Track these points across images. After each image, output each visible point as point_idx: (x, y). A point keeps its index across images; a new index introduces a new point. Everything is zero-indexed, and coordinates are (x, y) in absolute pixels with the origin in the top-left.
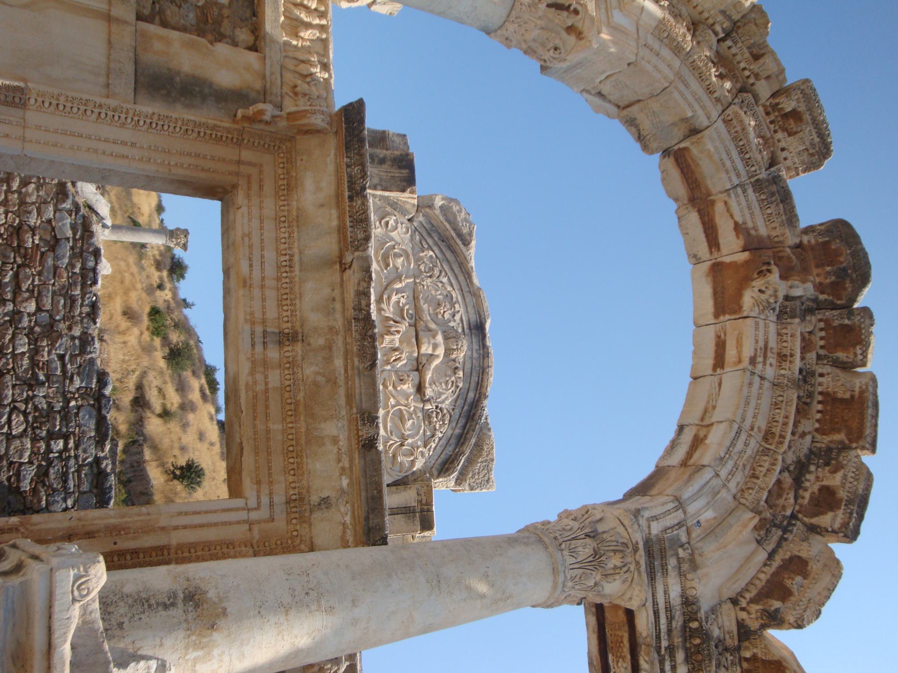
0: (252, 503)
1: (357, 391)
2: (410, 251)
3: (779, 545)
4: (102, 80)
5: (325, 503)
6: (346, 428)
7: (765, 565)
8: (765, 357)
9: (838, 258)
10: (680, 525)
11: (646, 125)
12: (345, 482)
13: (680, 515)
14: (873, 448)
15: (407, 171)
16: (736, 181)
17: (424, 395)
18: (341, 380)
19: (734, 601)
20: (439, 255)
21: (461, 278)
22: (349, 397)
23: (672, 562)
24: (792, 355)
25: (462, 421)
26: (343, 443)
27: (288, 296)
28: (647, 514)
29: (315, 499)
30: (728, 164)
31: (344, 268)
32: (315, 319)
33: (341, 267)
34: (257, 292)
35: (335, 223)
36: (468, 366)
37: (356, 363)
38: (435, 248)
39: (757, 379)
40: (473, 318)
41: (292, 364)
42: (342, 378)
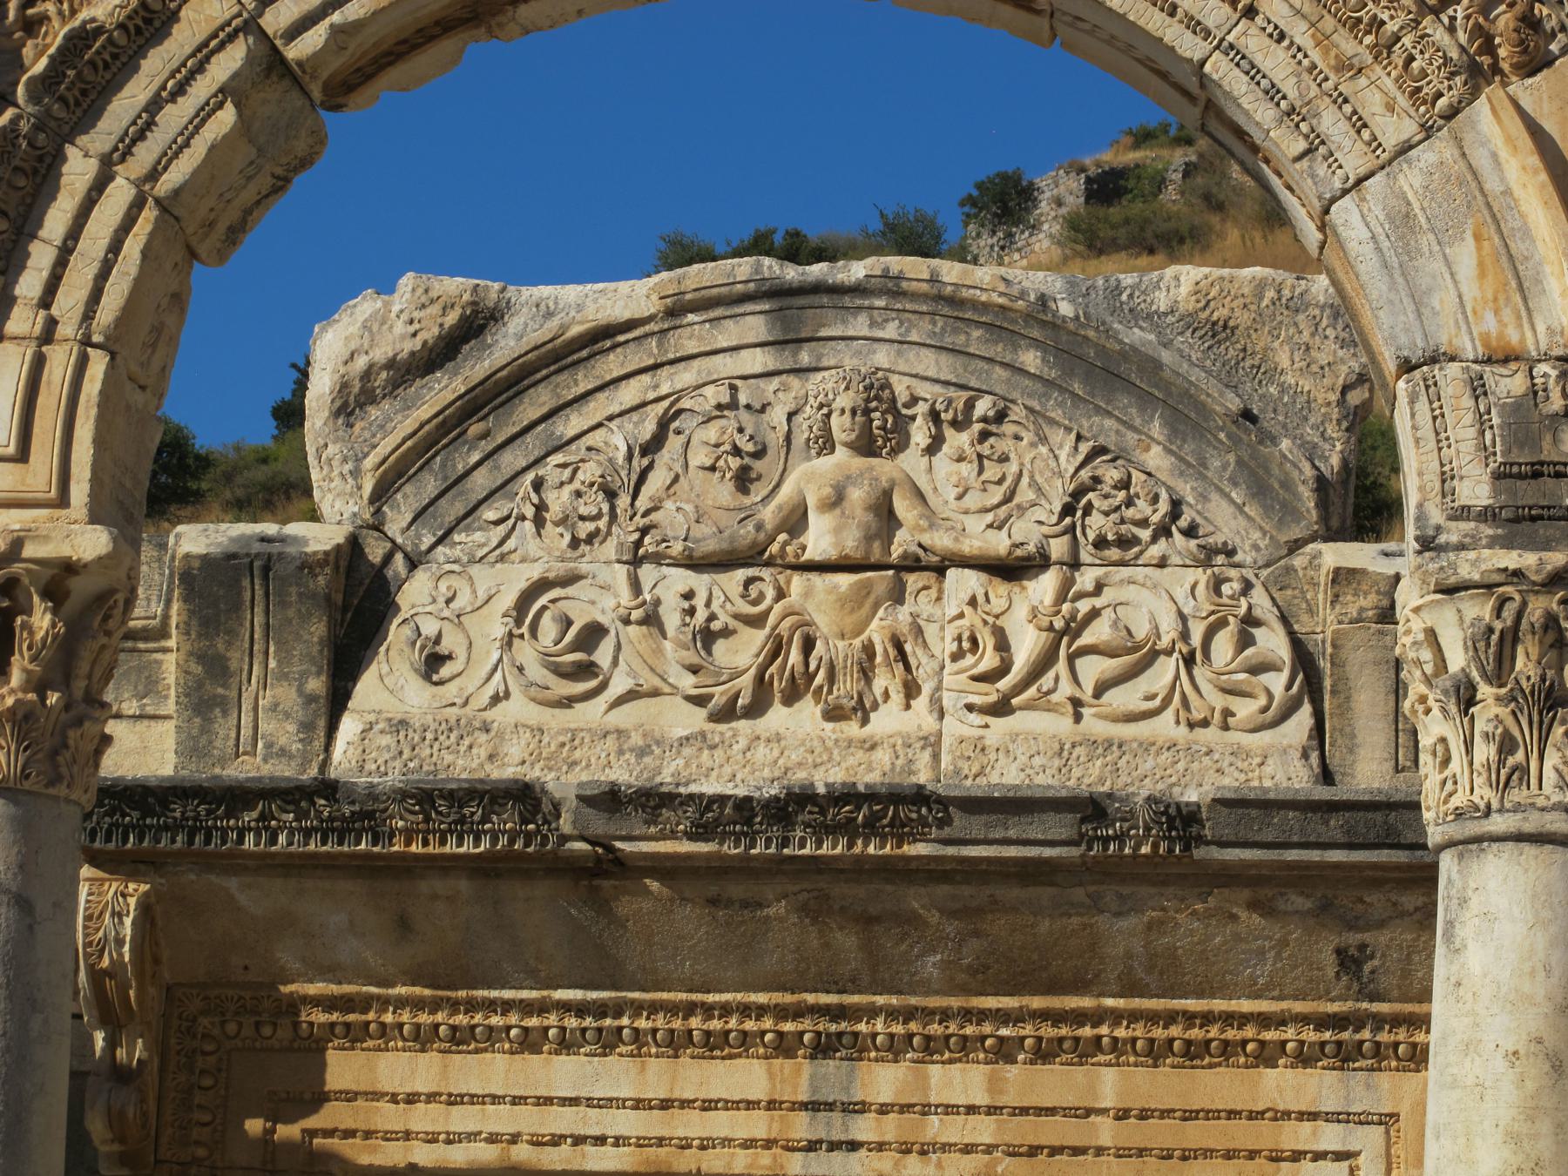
1: (1012, 852)
2: (535, 572)
6: (1126, 890)
10: (1478, 388)
11: (249, 195)
13: (1451, 377)
15: (246, 583)
17: (1029, 558)
20: (532, 445)
21: (612, 365)
28: (1436, 516)
33: (606, 874)
35: (463, 885)
36: (928, 362)
37: (921, 849)
38: (512, 459)
40: (754, 325)
42: (966, 891)
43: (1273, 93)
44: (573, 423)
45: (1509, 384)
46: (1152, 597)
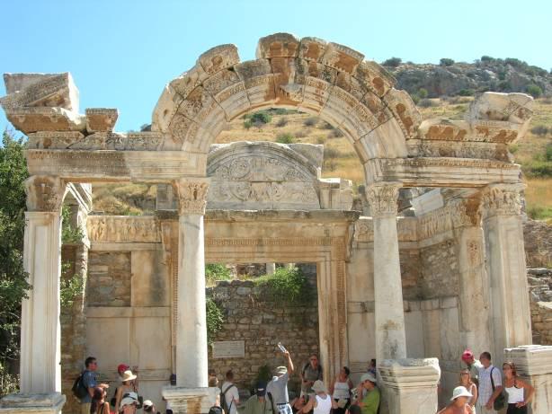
0: (323, 259)
3: (391, 110)
4: (161, 319)
5: (327, 231)
7: (398, 120)
8: (319, 96)
9: (280, 48)
10: (380, 162)
12: (320, 224)
13: (377, 161)
14: (362, 56)
16: (246, 99)
18: (280, 224)
19: (407, 139)
21: (227, 155)
22: (287, 221)
23: (392, 168)
24: (320, 83)
25: (293, 161)
26: (304, 225)
27: (243, 243)
29: (325, 235)
30: (240, 102)
31: (234, 221)
32: (254, 233)
34: (242, 255)
35: (214, 224)
39: (329, 104)
41: (271, 242)
43: (353, 124)
44: (222, 163)
45: (384, 161)
46: (298, 185)
